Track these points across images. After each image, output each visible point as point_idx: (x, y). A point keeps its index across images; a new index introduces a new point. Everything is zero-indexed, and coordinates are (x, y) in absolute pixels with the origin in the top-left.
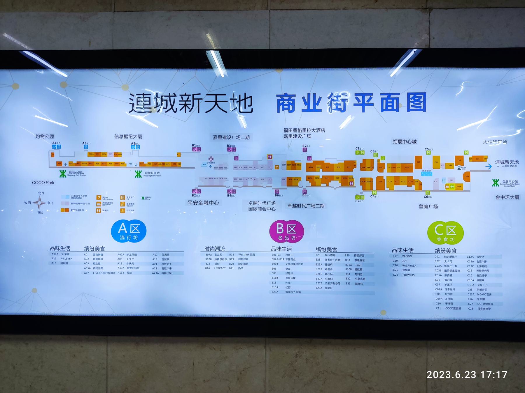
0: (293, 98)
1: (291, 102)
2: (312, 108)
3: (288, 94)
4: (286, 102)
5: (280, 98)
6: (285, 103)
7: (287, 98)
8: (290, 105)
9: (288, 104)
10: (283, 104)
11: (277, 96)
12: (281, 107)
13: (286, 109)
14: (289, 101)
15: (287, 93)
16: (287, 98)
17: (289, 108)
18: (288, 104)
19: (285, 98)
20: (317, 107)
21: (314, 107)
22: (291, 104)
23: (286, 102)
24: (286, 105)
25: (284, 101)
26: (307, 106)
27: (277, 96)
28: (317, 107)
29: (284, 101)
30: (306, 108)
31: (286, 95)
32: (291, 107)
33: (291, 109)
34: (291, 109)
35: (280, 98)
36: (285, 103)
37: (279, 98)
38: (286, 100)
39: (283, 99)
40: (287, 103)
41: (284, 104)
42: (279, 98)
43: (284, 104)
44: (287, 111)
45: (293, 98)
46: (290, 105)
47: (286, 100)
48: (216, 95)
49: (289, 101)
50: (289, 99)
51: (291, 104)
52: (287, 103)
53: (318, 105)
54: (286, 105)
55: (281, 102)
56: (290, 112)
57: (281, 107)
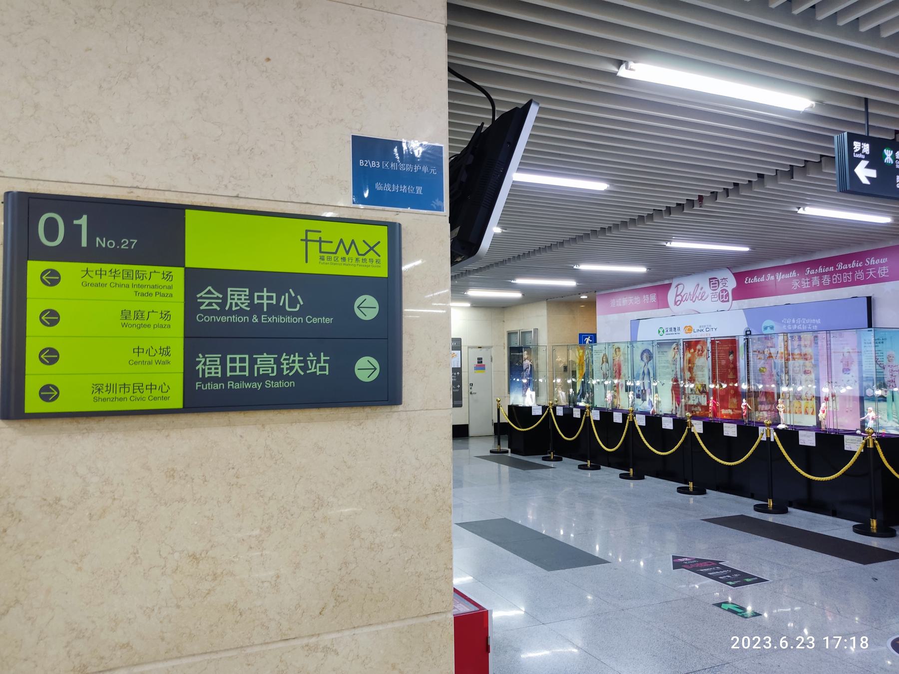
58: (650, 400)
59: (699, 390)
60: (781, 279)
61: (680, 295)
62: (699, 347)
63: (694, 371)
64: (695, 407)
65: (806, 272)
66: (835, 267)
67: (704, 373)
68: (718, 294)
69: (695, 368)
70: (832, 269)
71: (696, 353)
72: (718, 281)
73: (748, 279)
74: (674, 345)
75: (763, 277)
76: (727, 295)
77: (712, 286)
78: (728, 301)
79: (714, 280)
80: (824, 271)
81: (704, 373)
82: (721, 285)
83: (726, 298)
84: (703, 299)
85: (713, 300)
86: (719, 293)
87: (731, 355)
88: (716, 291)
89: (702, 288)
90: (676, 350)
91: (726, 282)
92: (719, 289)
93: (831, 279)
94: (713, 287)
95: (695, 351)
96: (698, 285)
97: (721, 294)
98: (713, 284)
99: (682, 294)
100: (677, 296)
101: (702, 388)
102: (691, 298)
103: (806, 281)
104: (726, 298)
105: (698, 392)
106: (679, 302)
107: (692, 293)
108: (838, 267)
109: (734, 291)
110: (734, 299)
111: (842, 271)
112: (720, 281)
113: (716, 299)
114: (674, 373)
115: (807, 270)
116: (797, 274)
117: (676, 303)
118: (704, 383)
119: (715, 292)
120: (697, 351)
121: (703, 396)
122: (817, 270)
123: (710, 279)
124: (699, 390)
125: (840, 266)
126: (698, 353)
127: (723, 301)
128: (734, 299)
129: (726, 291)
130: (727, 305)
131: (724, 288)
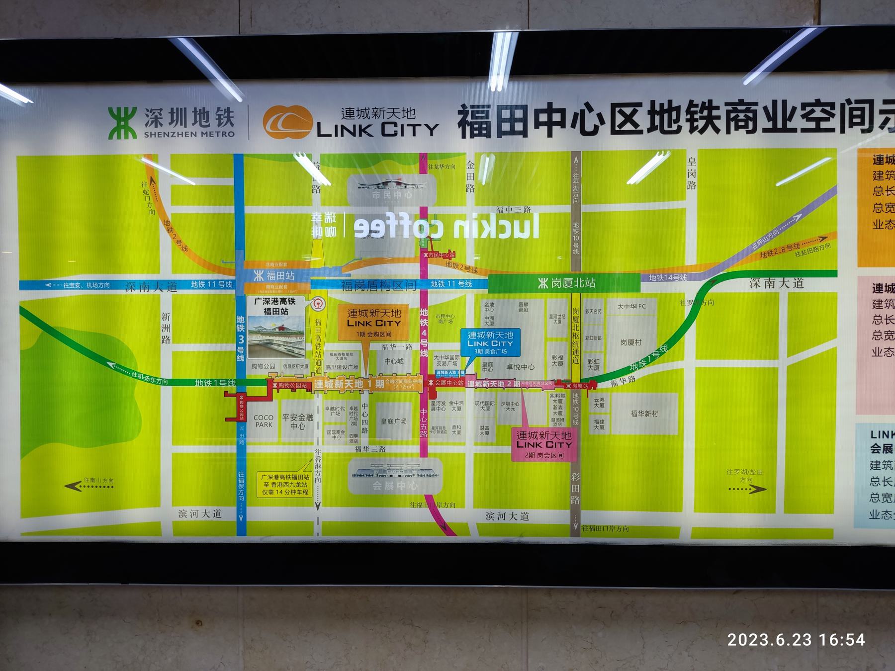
0: (753, 108)
1: (751, 115)
2: (780, 125)
3: (745, 101)
4: (742, 116)
5: (732, 109)
6: (739, 116)
7: (743, 108)
8: (749, 121)
9: (745, 118)
10: (736, 119)
11: (725, 105)
12: (733, 124)
13: (742, 127)
14: (747, 114)
15: (743, 100)
16: (743, 108)
17: (746, 126)
18: (745, 118)
19: (740, 108)
20: (790, 125)
21: (784, 124)
22: (750, 119)
23: (742, 116)
24: (742, 120)
25: (739, 114)
26: (771, 123)
27: (725, 105)
28: (790, 125)
29: (739, 114)
30: (770, 125)
31: (741, 102)
32: (751, 124)
33: (751, 127)
34: (751, 127)
35: (732, 109)
36: (739, 116)
37: (730, 108)
38: (741, 111)
39: (735, 110)
40: (744, 116)
41: (739, 118)
42: (730, 108)
43: (739, 118)
44: (742, 132)
45: (753, 108)
46: (749, 121)
47: (741, 111)
48: (394, 108)
49: (747, 114)
50: (748, 110)
51: (750, 119)
52: (744, 116)
53: (807, 121)
54: (742, 120)
55: (732, 115)
56: (748, 132)
57: (733, 124)
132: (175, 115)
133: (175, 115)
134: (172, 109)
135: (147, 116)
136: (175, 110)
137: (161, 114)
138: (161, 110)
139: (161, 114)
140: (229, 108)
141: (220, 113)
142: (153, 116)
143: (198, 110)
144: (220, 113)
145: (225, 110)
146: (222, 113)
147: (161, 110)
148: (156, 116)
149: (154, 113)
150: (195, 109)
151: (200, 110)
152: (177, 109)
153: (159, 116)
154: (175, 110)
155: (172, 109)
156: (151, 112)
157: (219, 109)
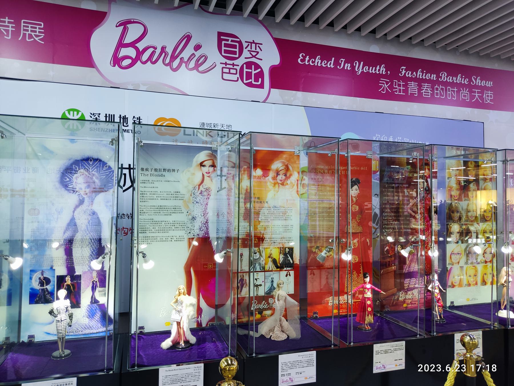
58: (94, 301)
59: (274, 261)
60: (363, 72)
61: (133, 45)
62: (277, 165)
63: (261, 217)
64: (259, 303)
65: (401, 73)
66: (438, 77)
67: (289, 222)
68: (238, 68)
69: (264, 212)
70: (434, 77)
71: (270, 178)
72: (240, 43)
73: (304, 57)
74: (202, 156)
75: (332, 62)
76: (260, 75)
77: (223, 48)
78: (261, 86)
79: (230, 39)
80: (424, 78)
81: (289, 222)
82: (246, 53)
83: (256, 80)
84: (201, 69)
85: (226, 76)
86: (242, 67)
87: (356, 187)
88: (236, 62)
89: (198, 47)
90: (205, 169)
91: (258, 50)
92: (241, 61)
93: (433, 90)
94: (226, 51)
95: (265, 175)
96: (188, 38)
97: (245, 70)
98: (226, 45)
99: (141, 46)
100: (121, 45)
101: (282, 256)
102: (168, 61)
103: (399, 85)
104: (256, 80)
105: (270, 265)
106: (129, 61)
107: (169, 50)
108: (441, 77)
109: (273, 70)
110: (274, 85)
111: (446, 84)
112: (245, 45)
113: (235, 77)
114: (198, 224)
115: (402, 69)
116: (386, 71)
117: (117, 61)
118: (287, 245)
119: (229, 62)
120: (271, 174)
121: (283, 273)
122: (414, 73)
123: (220, 34)
124: (274, 261)
125: (444, 77)
126: (274, 178)
127: (250, 85)
128: (274, 85)
129: (257, 66)
130: (260, 94)
131: (254, 60)
132: (108, 118)
133: (108, 118)
134: (106, 115)
135: (91, 117)
136: (108, 115)
137: (99, 117)
138: (99, 114)
139: (99, 117)
140: (139, 117)
141: (134, 119)
142: (95, 118)
143: (122, 116)
144: (134, 119)
145: (138, 118)
146: (136, 119)
147: (99, 114)
148: (96, 118)
149: (95, 116)
150: (120, 115)
151: (123, 117)
152: (109, 115)
153: (98, 118)
154: (108, 115)
155: (106, 115)
156: (93, 115)
157: (134, 117)
